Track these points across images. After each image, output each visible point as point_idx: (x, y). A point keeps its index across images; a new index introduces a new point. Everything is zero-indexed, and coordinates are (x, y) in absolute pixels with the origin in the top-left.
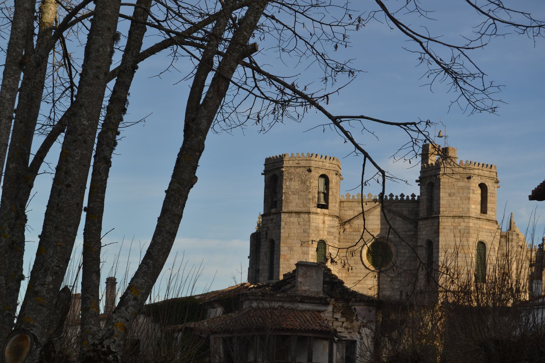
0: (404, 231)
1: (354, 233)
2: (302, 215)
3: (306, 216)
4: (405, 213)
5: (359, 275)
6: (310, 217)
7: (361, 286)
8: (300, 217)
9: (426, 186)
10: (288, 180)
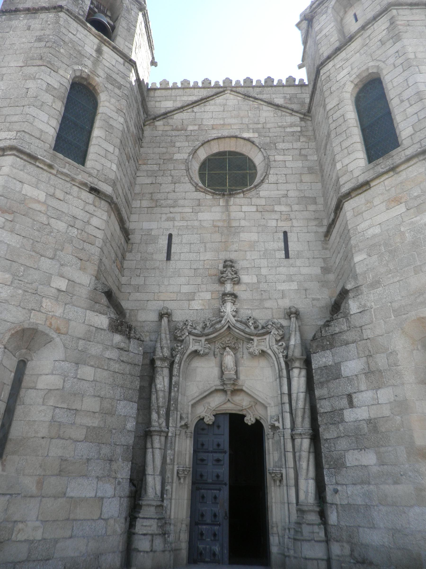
0: (279, 127)
1: (174, 133)
2: (43, 16)
3: (51, 15)
4: (279, 101)
5: (181, 202)
6: (59, 17)
7: (185, 224)
8: (35, 18)
9: (330, 11)
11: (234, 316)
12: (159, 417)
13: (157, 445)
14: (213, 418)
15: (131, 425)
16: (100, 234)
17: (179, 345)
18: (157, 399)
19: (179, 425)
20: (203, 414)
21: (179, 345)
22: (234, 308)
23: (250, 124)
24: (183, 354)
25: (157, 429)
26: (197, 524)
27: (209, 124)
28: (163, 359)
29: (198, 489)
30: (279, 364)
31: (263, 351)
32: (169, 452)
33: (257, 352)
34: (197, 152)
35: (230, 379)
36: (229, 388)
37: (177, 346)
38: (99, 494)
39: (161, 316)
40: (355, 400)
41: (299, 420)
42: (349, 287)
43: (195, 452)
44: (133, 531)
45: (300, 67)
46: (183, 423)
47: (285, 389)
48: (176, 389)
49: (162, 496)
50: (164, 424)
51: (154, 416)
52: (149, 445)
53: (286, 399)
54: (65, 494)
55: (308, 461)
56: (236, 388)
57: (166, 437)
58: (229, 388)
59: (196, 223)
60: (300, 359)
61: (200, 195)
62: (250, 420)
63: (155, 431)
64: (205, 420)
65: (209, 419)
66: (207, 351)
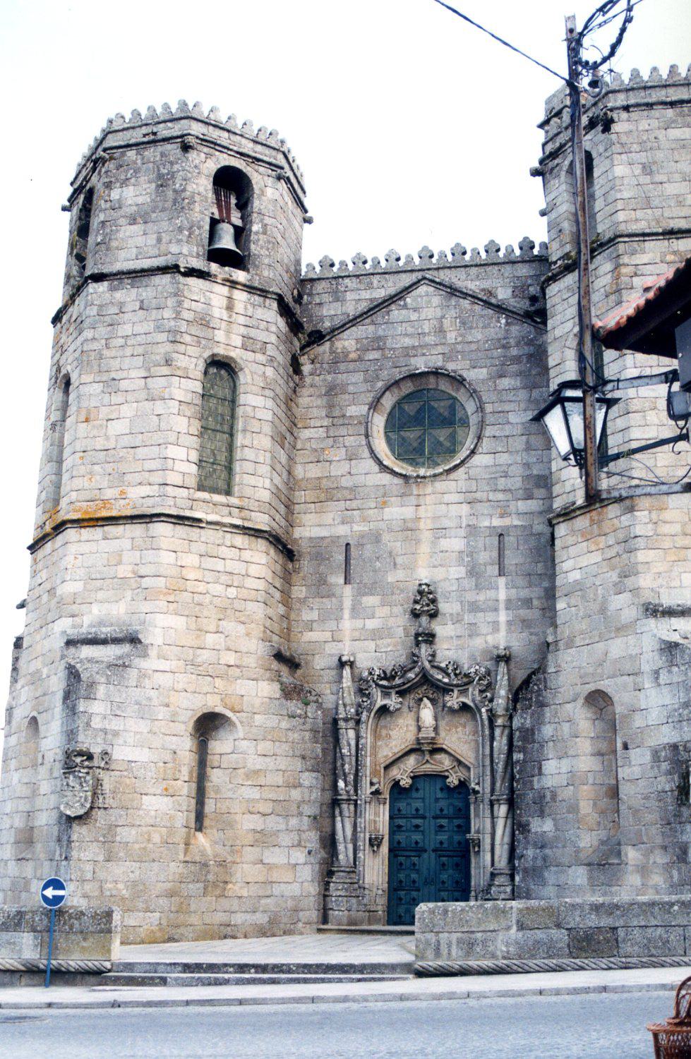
9: (563, 174)
10: (118, 185)
11: (430, 662)
12: (346, 786)
13: (346, 813)
14: (410, 781)
15: (316, 794)
16: (261, 585)
17: (365, 699)
18: (343, 765)
19: (369, 791)
20: (399, 777)
21: (365, 699)
22: (430, 651)
23: (458, 343)
24: (370, 711)
25: (345, 797)
26: (396, 890)
27: (397, 346)
28: (346, 720)
29: (396, 856)
30: (482, 720)
31: (464, 704)
32: (359, 820)
33: (456, 707)
34: (381, 401)
35: (427, 738)
36: (426, 747)
37: (363, 701)
38: (293, 861)
39: (342, 664)
40: (543, 768)
41: (498, 785)
42: (550, 639)
43: (391, 818)
44: (327, 893)
45: (543, 214)
46: (374, 789)
47: (487, 751)
48: (363, 753)
49: (355, 863)
50: (352, 792)
51: (341, 784)
52: (337, 812)
53: (488, 762)
54: (261, 861)
55: (505, 826)
56: (435, 746)
57: (356, 805)
58: (426, 747)
59: (382, 525)
60: (503, 715)
61: (386, 478)
62: (453, 780)
63: (343, 800)
64: (401, 783)
65: (406, 782)
66: (399, 706)
